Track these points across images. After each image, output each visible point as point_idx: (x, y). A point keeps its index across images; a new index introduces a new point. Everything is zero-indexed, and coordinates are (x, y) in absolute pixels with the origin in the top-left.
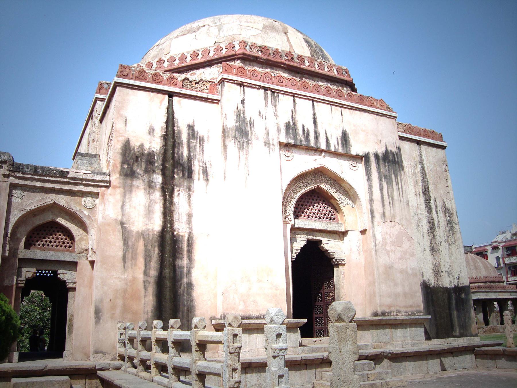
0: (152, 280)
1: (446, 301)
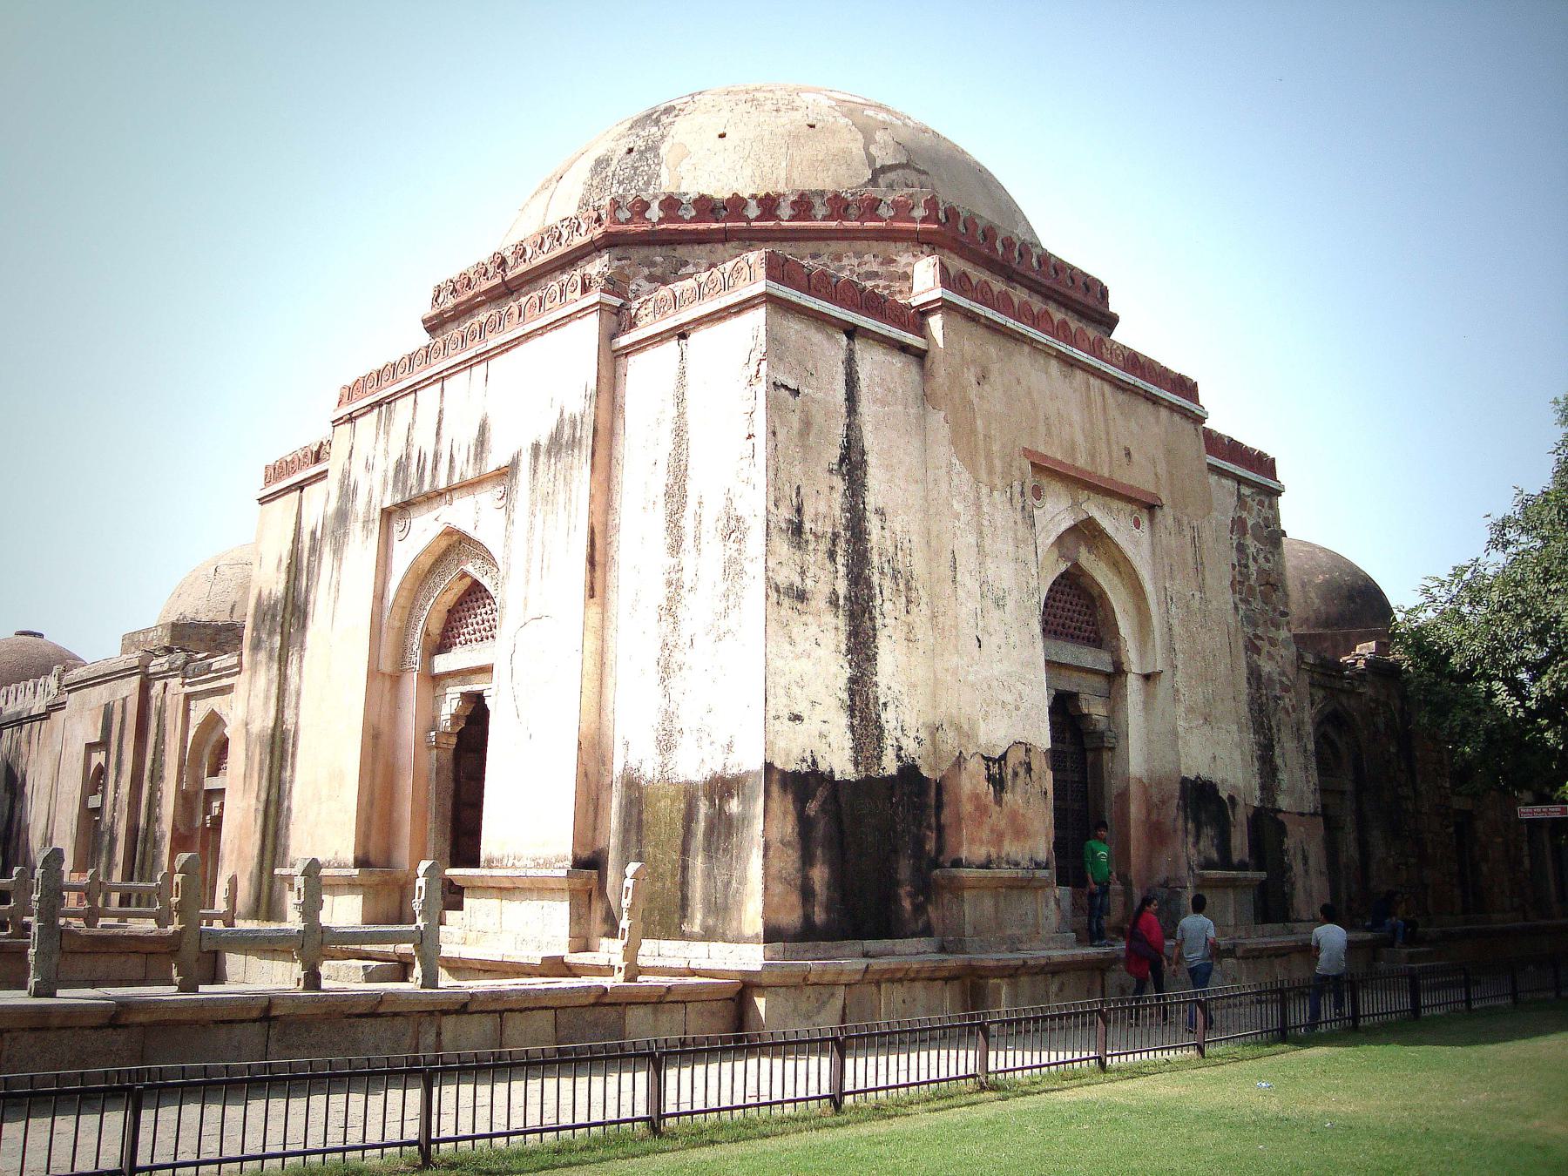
0: (261, 807)
1: (679, 825)
